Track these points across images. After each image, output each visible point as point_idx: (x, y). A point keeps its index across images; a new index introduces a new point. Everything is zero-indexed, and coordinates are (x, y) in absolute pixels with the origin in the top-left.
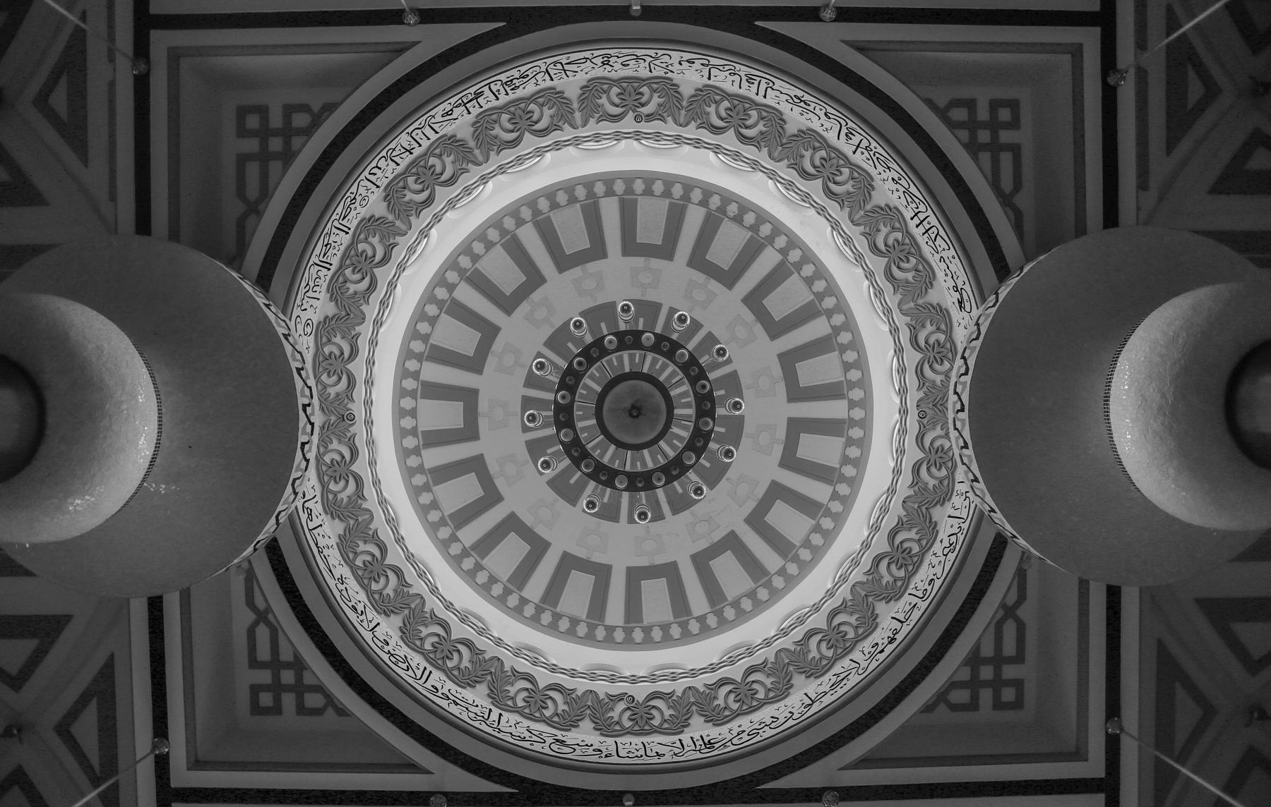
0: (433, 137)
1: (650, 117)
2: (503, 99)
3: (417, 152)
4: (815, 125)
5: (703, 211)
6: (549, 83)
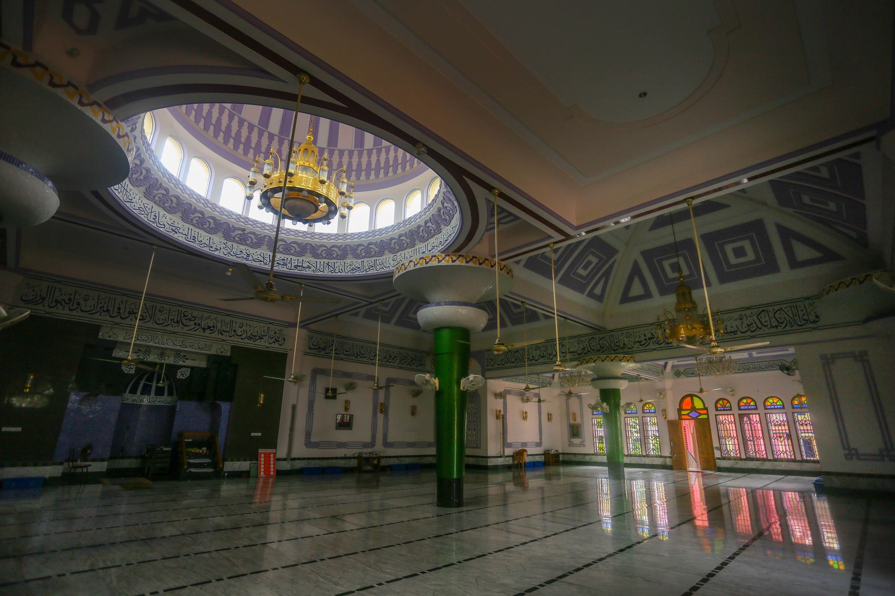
0: (318, 261)
1: (239, 229)
2: (289, 257)
3: (326, 261)
4: (168, 216)
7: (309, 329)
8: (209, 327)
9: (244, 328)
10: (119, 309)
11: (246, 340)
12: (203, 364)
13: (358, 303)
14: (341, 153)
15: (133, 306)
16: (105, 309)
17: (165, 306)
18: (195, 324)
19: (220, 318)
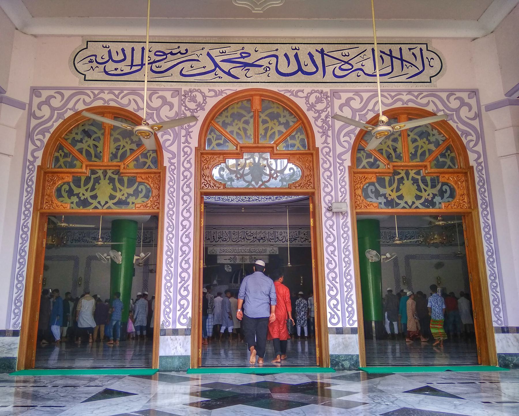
8: (262, 238)
9: (283, 235)
10: (214, 237)
15: (220, 234)
17: (235, 230)
18: (254, 238)
19: (267, 231)
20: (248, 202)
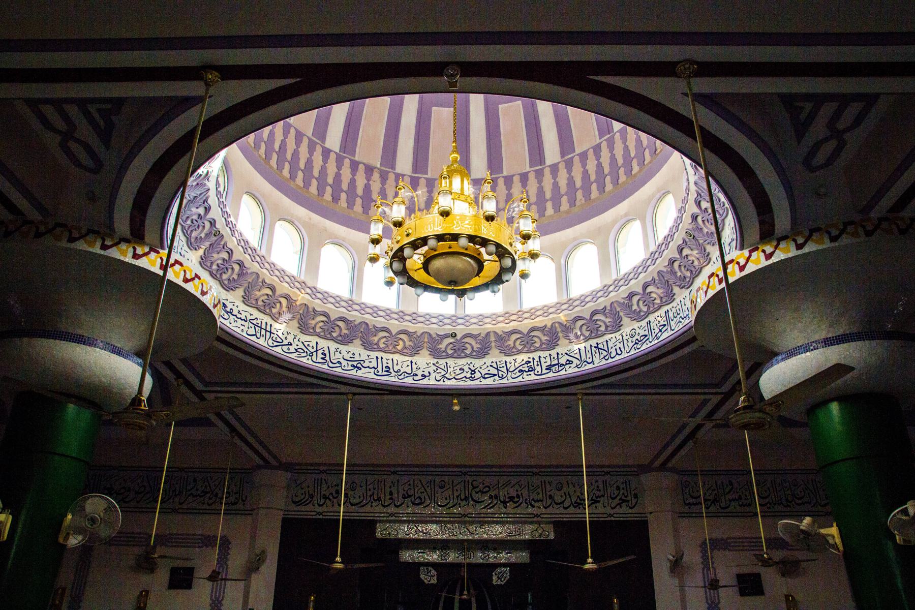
1: (446, 336)
2: (536, 355)
4: (343, 348)
5: (398, 170)
6: (508, 359)
7: (673, 470)
8: (511, 499)
9: (565, 490)
10: (391, 493)
11: (572, 510)
12: (522, 557)
13: (705, 402)
14: (584, 156)
16: (463, 497)
17: (446, 479)
18: (491, 497)
20: (470, 383)
